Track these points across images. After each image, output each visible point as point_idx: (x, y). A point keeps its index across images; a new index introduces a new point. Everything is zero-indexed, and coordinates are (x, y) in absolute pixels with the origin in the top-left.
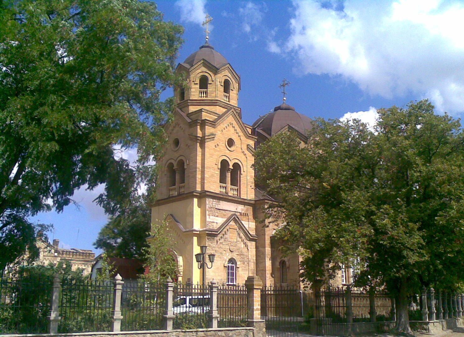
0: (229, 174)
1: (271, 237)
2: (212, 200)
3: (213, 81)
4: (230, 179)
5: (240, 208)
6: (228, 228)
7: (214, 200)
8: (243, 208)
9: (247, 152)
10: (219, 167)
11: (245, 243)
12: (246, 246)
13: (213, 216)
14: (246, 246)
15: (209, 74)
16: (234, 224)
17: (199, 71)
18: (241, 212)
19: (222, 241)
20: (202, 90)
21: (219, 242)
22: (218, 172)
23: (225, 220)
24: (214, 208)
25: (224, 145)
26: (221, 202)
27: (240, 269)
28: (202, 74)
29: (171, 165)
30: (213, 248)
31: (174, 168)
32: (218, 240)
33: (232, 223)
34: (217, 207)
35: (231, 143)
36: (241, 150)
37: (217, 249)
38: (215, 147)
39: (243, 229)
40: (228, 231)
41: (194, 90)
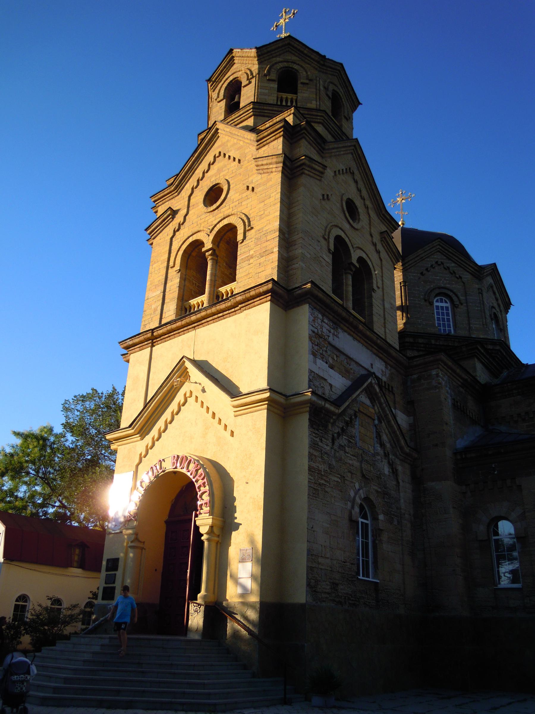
0: (350, 277)
1: (455, 454)
2: (320, 316)
3: (311, 80)
4: (350, 289)
5: (378, 367)
6: (357, 410)
7: (326, 321)
8: (384, 369)
9: (380, 247)
10: (332, 247)
11: (391, 465)
12: (394, 472)
13: (322, 358)
14: (394, 472)
15: (301, 66)
16: (367, 402)
17: (278, 59)
18: (380, 376)
19: (343, 440)
20: (284, 95)
21: (336, 443)
22: (328, 258)
23: (348, 383)
24: (325, 340)
25: (338, 205)
26: (340, 330)
27: (385, 537)
28: (286, 64)
29: (198, 244)
30: (325, 457)
31: (204, 250)
32: (335, 435)
33: (364, 399)
34: (330, 339)
35: (351, 209)
36: (370, 238)
37: (334, 463)
38: (322, 198)
39: (389, 422)
40: (356, 417)
41: (267, 91)
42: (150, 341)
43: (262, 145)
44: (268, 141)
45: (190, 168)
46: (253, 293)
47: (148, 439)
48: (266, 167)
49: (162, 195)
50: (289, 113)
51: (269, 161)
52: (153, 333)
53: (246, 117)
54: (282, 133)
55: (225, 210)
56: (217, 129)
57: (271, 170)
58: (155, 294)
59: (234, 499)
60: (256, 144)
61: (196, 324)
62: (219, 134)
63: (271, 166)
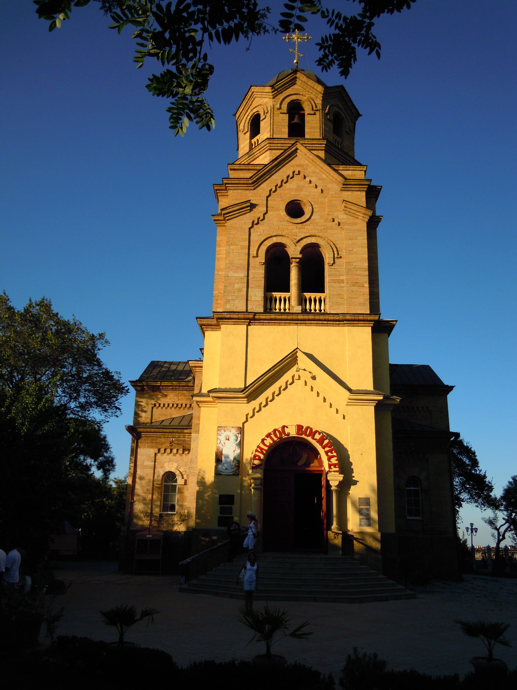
20: (336, 137)
42: (248, 321)
43: (346, 189)
44: (352, 189)
45: (268, 171)
46: (361, 318)
47: (255, 404)
48: (353, 212)
49: (237, 182)
50: (361, 169)
51: (360, 210)
52: (254, 315)
53: (317, 148)
54: (366, 189)
55: (309, 229)
56: (297, 149)
57: (358, 216)
58: (236, 275)
59: (351, 464)
60: (342, 186)
61: (299, 322)
62: (298, 154)
63: (359, 214)
